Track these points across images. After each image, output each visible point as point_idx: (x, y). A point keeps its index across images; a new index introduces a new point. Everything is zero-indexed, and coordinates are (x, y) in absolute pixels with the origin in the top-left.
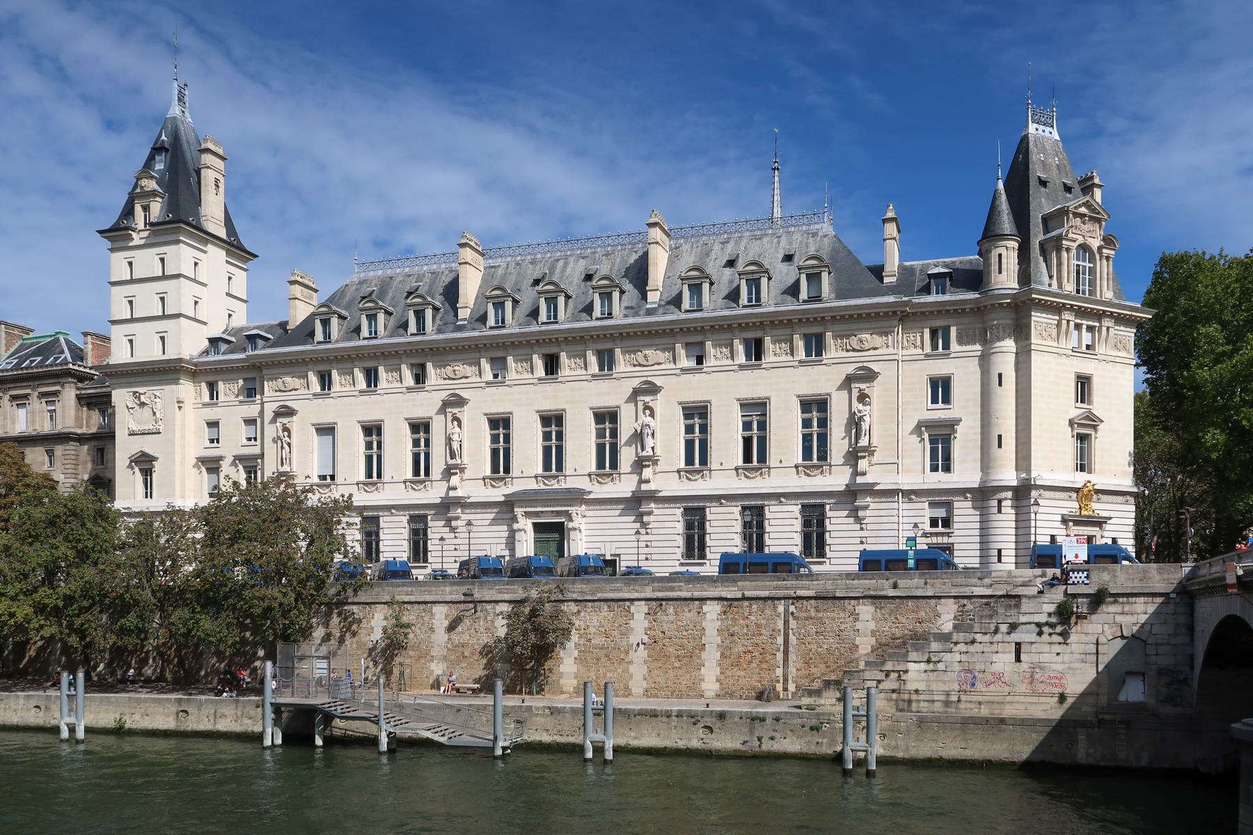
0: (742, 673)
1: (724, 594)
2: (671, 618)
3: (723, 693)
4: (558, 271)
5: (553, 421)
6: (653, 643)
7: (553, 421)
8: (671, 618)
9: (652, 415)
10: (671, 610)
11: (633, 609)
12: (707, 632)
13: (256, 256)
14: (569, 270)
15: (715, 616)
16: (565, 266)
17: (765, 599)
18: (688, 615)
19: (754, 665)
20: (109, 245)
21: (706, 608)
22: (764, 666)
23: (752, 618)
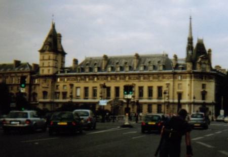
5: (117, 89)
7: (117, 89)
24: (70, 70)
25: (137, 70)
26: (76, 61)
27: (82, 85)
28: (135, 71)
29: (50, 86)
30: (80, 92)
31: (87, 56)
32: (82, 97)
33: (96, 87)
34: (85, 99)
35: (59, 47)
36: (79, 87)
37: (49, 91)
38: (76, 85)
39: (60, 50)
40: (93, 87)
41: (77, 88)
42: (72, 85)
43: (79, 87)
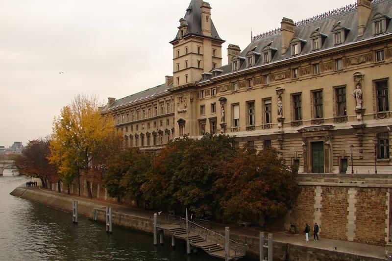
0: (367, 229)
1: (358, 185)
2: (333, 196)
3: (357, 239)
4: (323, 27)
5: (317, 95)
6: (324, 210)
7: (317, 95)
8: (333, 196)
9: (360, 88)
10: (333, 192)
11: (315, 191)
12: (350, 205)
13: (224, 41)
14: (328, 25)
15: (354, 196)
16: (327, 24)
17: (380, 188)
18: (341, 196)
19: (373, 225)
20: (172, 46)
21: (350, 192)
22: (378, 226)
23: (373, 198)
24: (226, 69)
25: (367, 36)
26: (233, 49)
27: (242, 97)
28: (359, 38)
29: (188, 109)
30: (240, 113)
31: (255, 35)
32: (243, 124)
33: (270, 99)
34: (248, 129)
35: (205, 26)
36: (238, 104)
37: (186, 118)
38: (231, 99)
39: (209, 35)
40: (264, 100)
41: (234, 105)
42: (223, 101)
43: (238, 104)
